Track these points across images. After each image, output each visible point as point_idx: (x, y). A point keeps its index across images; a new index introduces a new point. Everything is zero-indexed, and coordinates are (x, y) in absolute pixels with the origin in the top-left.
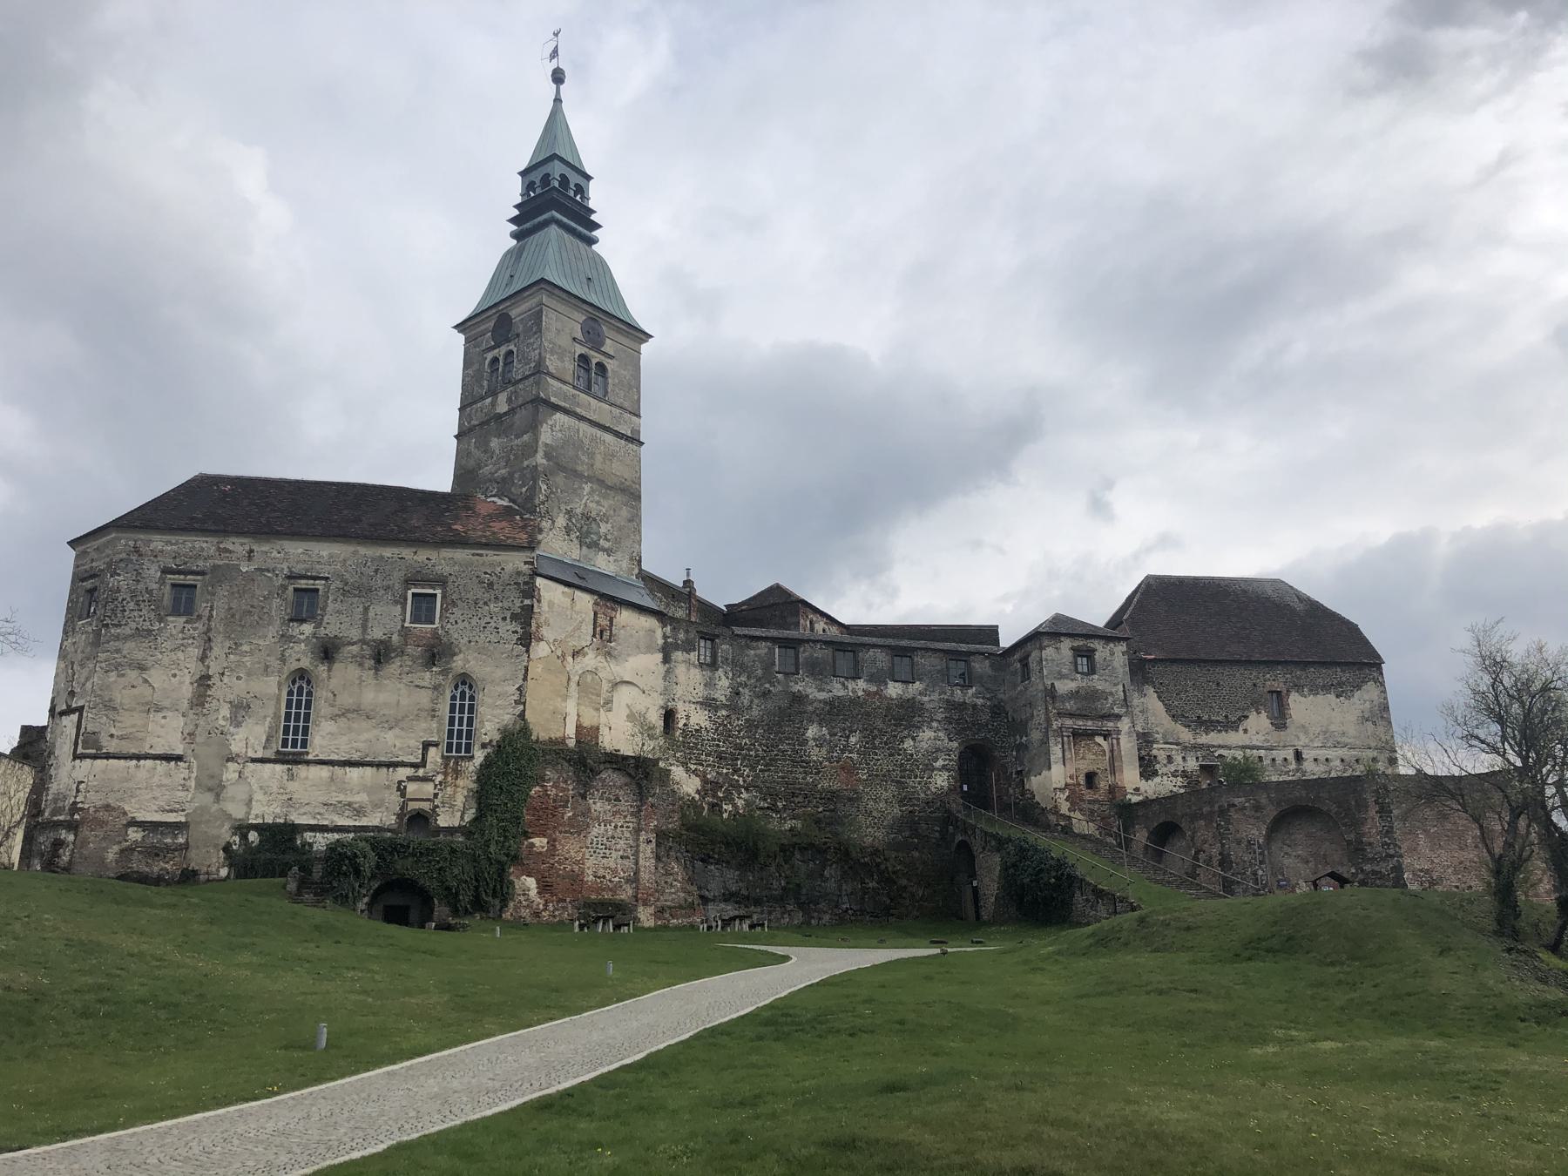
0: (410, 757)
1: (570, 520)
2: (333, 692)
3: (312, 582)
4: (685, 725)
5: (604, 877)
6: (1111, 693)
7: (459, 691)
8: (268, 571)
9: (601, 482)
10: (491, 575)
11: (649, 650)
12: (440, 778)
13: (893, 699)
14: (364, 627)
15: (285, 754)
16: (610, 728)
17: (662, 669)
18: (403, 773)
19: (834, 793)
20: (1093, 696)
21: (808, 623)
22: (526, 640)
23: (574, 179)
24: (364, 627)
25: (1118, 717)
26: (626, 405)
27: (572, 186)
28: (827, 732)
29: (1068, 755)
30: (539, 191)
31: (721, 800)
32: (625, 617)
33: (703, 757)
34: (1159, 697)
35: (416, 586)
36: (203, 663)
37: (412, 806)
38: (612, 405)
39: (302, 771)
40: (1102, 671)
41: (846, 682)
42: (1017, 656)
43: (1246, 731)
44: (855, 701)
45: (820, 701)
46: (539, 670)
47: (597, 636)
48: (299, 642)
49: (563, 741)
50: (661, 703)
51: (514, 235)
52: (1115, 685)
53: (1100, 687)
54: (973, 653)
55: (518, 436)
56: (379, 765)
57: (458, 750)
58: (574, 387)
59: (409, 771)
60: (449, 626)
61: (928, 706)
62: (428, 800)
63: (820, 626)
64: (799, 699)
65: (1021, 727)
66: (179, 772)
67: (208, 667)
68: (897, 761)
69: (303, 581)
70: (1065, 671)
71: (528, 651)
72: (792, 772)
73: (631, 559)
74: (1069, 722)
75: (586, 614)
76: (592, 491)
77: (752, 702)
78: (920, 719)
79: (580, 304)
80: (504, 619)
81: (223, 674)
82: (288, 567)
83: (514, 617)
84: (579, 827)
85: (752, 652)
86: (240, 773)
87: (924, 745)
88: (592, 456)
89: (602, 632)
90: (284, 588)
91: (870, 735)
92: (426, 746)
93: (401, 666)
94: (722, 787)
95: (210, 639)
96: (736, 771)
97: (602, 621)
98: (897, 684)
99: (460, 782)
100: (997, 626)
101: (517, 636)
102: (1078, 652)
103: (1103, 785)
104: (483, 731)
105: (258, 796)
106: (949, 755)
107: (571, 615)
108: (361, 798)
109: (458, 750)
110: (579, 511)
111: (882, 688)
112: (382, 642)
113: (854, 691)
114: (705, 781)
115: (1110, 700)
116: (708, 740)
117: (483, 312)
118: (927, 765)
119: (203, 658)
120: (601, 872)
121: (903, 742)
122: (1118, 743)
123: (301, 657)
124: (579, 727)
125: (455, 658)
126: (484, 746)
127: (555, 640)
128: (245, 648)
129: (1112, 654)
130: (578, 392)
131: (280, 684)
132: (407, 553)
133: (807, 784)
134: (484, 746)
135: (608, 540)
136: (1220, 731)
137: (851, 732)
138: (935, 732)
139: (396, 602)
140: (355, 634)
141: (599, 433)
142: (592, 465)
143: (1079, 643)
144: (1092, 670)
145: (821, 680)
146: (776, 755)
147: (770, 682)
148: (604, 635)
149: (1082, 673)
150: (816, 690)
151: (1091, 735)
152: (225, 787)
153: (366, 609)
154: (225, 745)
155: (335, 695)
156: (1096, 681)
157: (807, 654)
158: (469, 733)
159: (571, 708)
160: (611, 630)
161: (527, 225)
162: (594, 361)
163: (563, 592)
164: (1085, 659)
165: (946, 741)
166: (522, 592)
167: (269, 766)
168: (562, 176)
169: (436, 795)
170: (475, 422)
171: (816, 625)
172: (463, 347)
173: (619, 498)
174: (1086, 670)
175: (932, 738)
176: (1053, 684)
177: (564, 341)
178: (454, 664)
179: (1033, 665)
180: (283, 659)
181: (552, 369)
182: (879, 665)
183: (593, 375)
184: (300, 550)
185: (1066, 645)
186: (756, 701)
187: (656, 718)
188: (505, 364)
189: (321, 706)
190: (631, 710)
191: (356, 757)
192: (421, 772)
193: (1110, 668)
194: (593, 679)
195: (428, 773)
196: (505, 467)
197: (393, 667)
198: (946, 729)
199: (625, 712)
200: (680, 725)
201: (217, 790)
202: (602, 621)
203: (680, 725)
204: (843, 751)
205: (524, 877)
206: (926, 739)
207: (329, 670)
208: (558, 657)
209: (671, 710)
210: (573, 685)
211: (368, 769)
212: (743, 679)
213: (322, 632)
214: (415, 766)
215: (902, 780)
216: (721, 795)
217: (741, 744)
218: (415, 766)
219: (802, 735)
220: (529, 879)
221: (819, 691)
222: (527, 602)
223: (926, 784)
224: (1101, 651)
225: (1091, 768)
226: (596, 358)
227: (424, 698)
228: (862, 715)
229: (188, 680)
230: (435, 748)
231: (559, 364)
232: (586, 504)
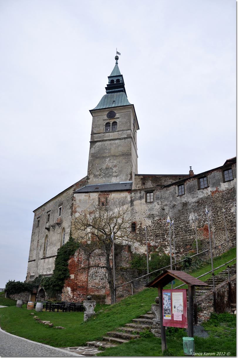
4: (140, 227)
19: (202, 241)
28: (197, 215)
38: (118, 131)
44: (207, 198)
45: (194, 203)
64: (185, 204)
72: (185, 236)
73: (127, 175)
76: (110, 160)
79: (104, 110)
85: (168, 192)
91: (216, 211)
94: (158, 247)
96: (164, 240)
107: (89, 201)
113: (207, 193)
114: (149, 246)
116: (150, 230)
130: (104, 134)
133: (191, 239)
142: (110, 152)
145: (193, 193)
146: (179, 230)
147: (175, 201)
150: (192, 198)
157: (188, 184)
163: (85, 195)
173: (121, 158)
186: (171, 210)
200: (138, 227)
204: (204, 222)
205: (68, 287)
209: (134, 223)
216: (157, 250)
217: (166, 229)
219: (188, 219)
220: (69, 288)
221: (193, 198)
228: (211, 203)
232: (107, 164)
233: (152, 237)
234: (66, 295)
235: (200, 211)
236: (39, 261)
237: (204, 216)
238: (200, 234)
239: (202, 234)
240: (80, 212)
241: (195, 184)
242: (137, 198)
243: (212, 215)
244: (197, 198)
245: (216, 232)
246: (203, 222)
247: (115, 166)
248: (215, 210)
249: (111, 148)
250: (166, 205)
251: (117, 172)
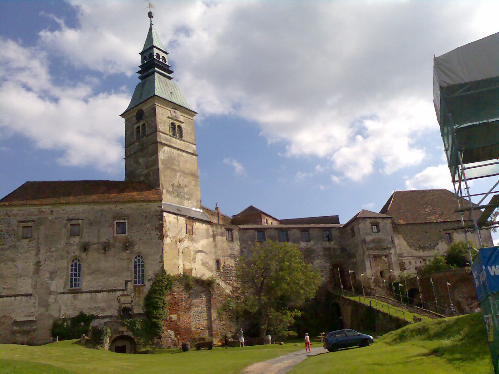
0: (121, 287)
1: (173, 187)
2: (88, 264)
3: (77, 221)
5: (199, 328)
6: (387, 239)
7: (137, 259)
8: (60, 218)
9: (184, 172)
10: (146, 212)
11: (207, 238)
12: (133, 294)
14: (99, 237)
15: (72, 290)
16: (196, 269)
17: (213, 244)
18: (119, 293)
20: (380, 241)
21: (265, 220)
22: (162, 237)
23: (161, 54)
24: (99, 237)
25: (390, 248)
26: (190, 140)
27: (161, 57)
29: (373, 265)
30: (148, 61)
31: (240, 294)
32: (197, 225)
33: (231, 278)
34: (404, 239)
35: (117, 219)
36: (37, 257)
37: (123, 306)
38: (184, 141)
39: (79, 295)
42: (349, 227)
43: (438, 250)
46: (167, 248)
47: (188, 233)
48: (73, 245)
49: (179, 275)
50: (214, 257)
51: (140, 78)
52: (388, 236)
54: (332, 228)
55: (151, 157)
56: (109, 291)
57: (139, 283)
58: (170, 136)
59: (121, 293)
60: (132, 234)
61: (317, 250)
62: (129, 303)
63: (270, 221)
65: (351, 256)
66: (32, 300)
67: (39, 258)
69: (73, 221)
70: (368, 232)
71: (163, 241)
73: (197, 201)
74: (372, 252)
75: (183, 225)
76: (180, 176)
77: (248, 254)
80: (153, 230)
81: (45, 260)
82: (67, 216)
83: (156, 228)
84: (187, 310)
86: (55, 299)
88: (179, 162)
89: (189, 231)
90: (66, 224)
92: (127, 282)
93: (114, 251)
95: (39, 247)
97: (189, 227)
98: (304, 242)
99: (141, 295)
100: (338, 216)
101: (158, 236)
102: (373, 224)
103: (387, 275)
104: (148, 274)
105: (63, 307)
108: (102, 305)
109: (139, 283)
110: (176, 184)
112: (106, 243)
114: (233, 287)
115: (386, 242)
117: (132, 109)
119: (37, 254)
120: (198, 326)
122: (391, 259)
123: (75, 251)
124: (184, 269)
125: (135, 246)
126: (149, 280)
127: (173, 236)
128: (53, 249)
129: (386, 224)
131: (68, 263)
132: (112, 206)
134: (149, 280)
135: (187, 195)
136: (428, 251)
138: (320, 260)
139: (111, 227)
140: (95, 240)
141: (181, 153)
143: (373, 220)
144: (378, 231)
148: (190, 232)
149: (375, 232)
151: (379, 256)
152: (49, 305)
153: (99, 231)
154: (48, 288)
155: (90, 265)
156: (380, 235)
158: (143, 276)
159: (180, 262)
160: (193, 230)
161: (145, 74)
162: (177, 125)
164: (376, 227)
165: (325, 263)
166: (159, 218)
167: (66, 295)
168: (157, 54)
169: (132, 301)
170: (132, 152)
171: (268, 221)
172: (124, 123)
174: (376, 231)
176: (364, 238)
177: (165, 118)
178: (135, 249)
179: (356, 230)
180: (68, 253)
181: (161, 130)
183: (177, 130)
184: (71, 209)
185: (368, 221)
187: (212, 263)
188: (142, 129)
189: (84, 269)
190: (203, 262)
191: (100, 289)
192: (126, 293)
194: (188, 250)
195: (128, 293)
196: (146, 169)
197: (111, 252)
198: (324, 259)
199: (200, 262)
200: (222, 266)
201: (46, 305)
202: (189, 227)
203: (222, 266)
207: (87, 255)
208: (174, 243)
210: (181, 254)
211: (105, 293)
212: (244, 245)
213: (83, 241)
214: (122, 290)
218: (122, 290)
222: (161, 222)
224: (382, 223)
225: (382, 270)
226: (177, 124)
227: (125, 263)
229: (31, 264)
230: (130, 283)
231: (164, 127)
232: (178, 181)
233: (235, 278)
234: (168, 340)
236: (52, 296)
240: (171, 237)
242: (219, 233)
247: (186, 186)
249: (180, 161)
250: (245, 248)
251: (188, 195)
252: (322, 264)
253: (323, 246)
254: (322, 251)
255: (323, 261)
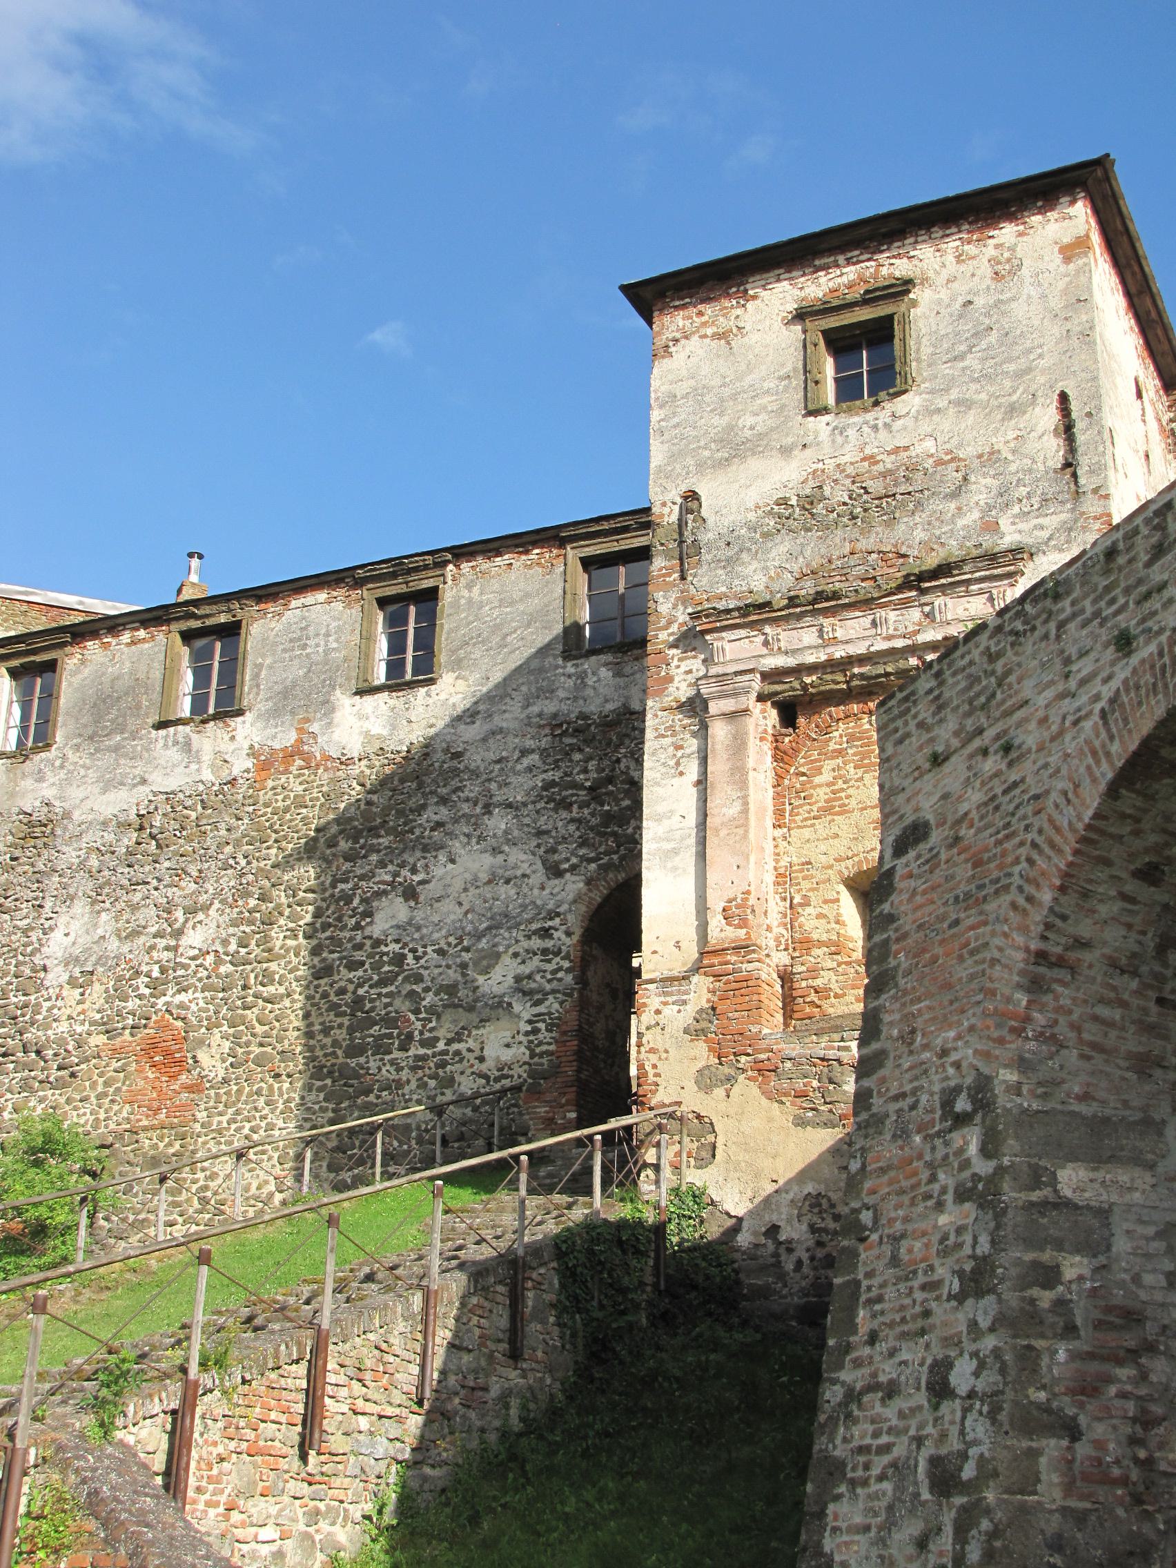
13: (347, 762)
40: (946, 370)
41: (194, 737)
45: (105, 824)
52: (1013, 410)
53: (929, 445)
61: (476, 758)
68: (342, 991)
70: (751, 421)
78: (444, 813)
87: (450, 912)
106: (545, 933)
111: (315, 727)
115: (982, 489)
118: (451, 989)
121: (368, 914)
137: (191, 911)
138: (496, 851)
145: (116, 749)
165: (539, 876)
175: (484, 877)
176: (692, 496)
182: (316, 647)
193: (993, 338)
198: (540, 833)
204: (156, 986)
206: (458, 885)
215: (353, 1063)
221: (104, 791)
223: (443, 1065)
235: (137, 897)
237: (162, 943)
238: (107, 1084)
239: (118, 1090)
241: (141, 676)
243: (225, 942)
244: (144, 790)
245: (225, 1081)
246: (147, 991)
248: (252, 902)
252: (506, 891)
253: (550, 707)
254: (534, 758)
255: (521, 858)
